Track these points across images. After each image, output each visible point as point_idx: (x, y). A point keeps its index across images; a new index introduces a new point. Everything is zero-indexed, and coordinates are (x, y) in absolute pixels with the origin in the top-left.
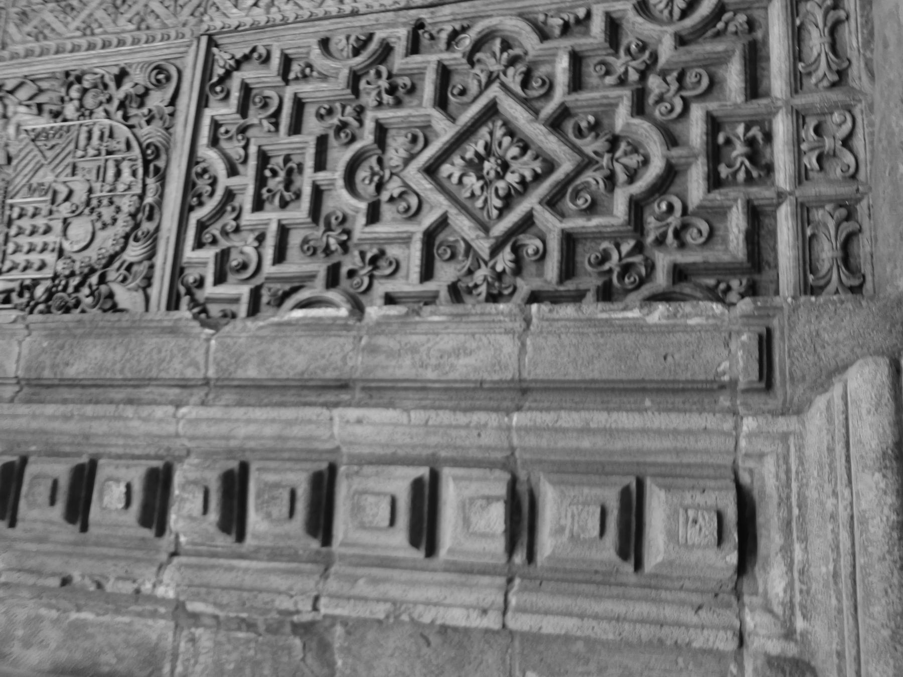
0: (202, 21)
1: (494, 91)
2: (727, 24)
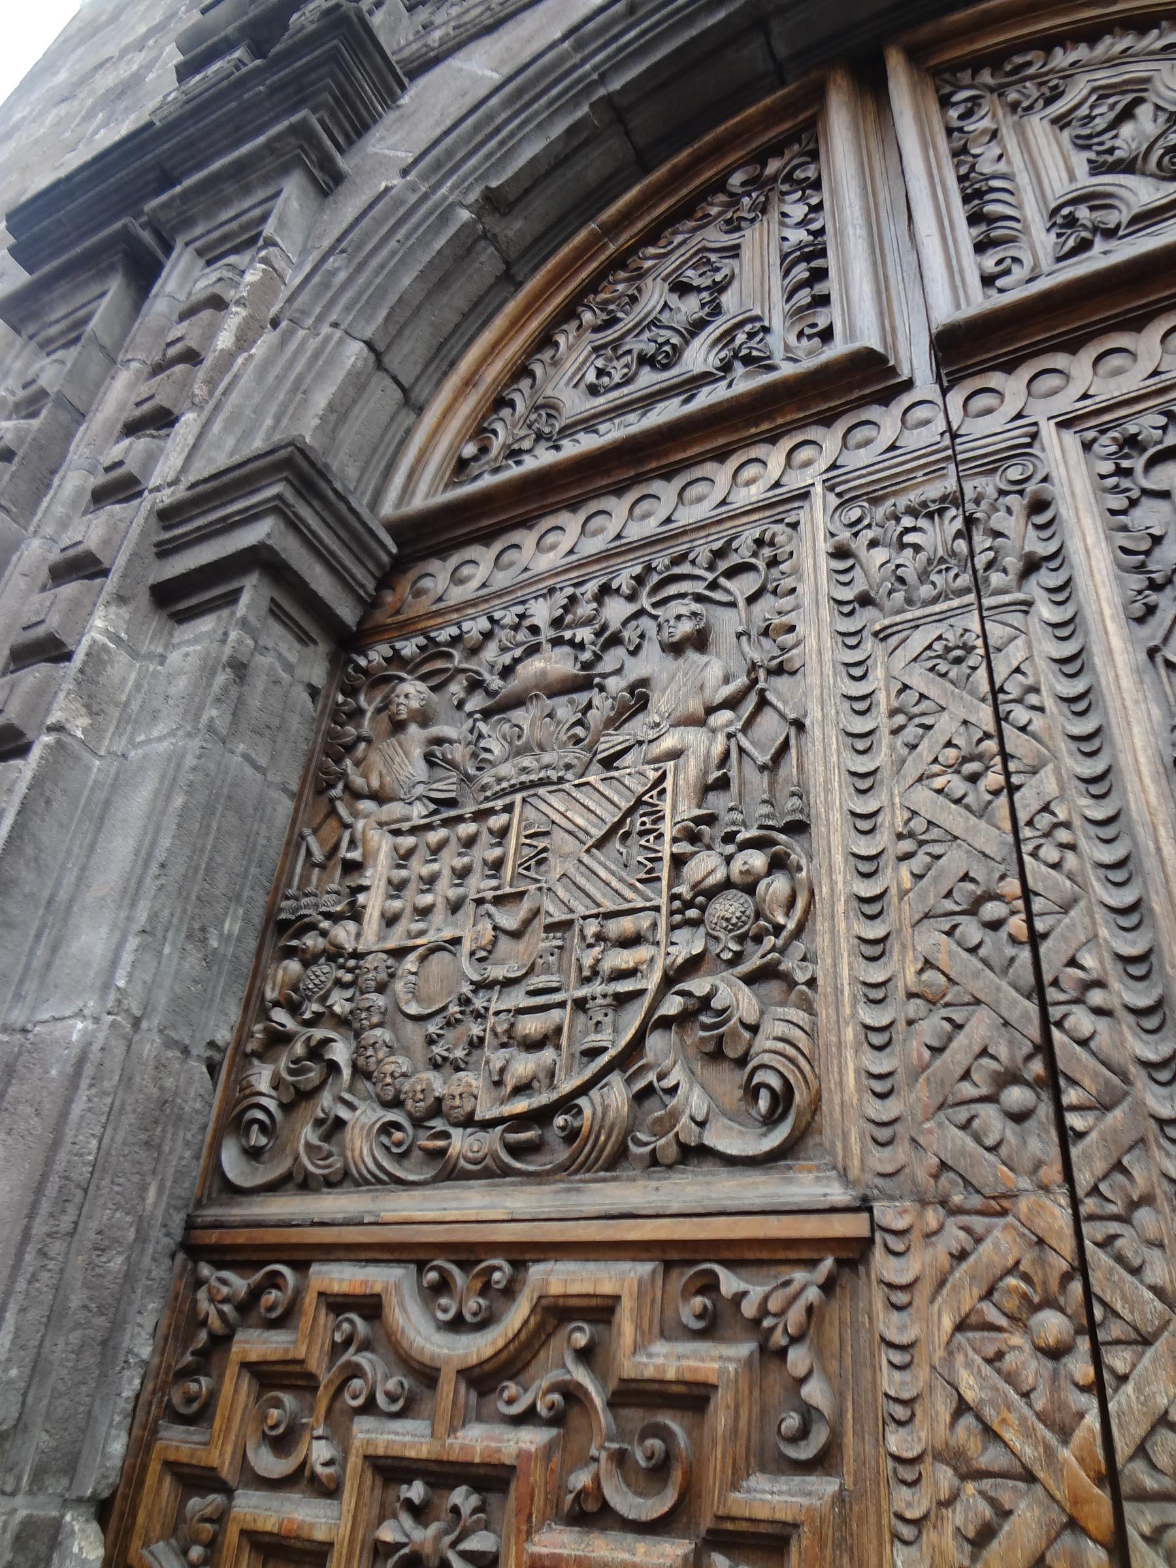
0: (924, 1203)
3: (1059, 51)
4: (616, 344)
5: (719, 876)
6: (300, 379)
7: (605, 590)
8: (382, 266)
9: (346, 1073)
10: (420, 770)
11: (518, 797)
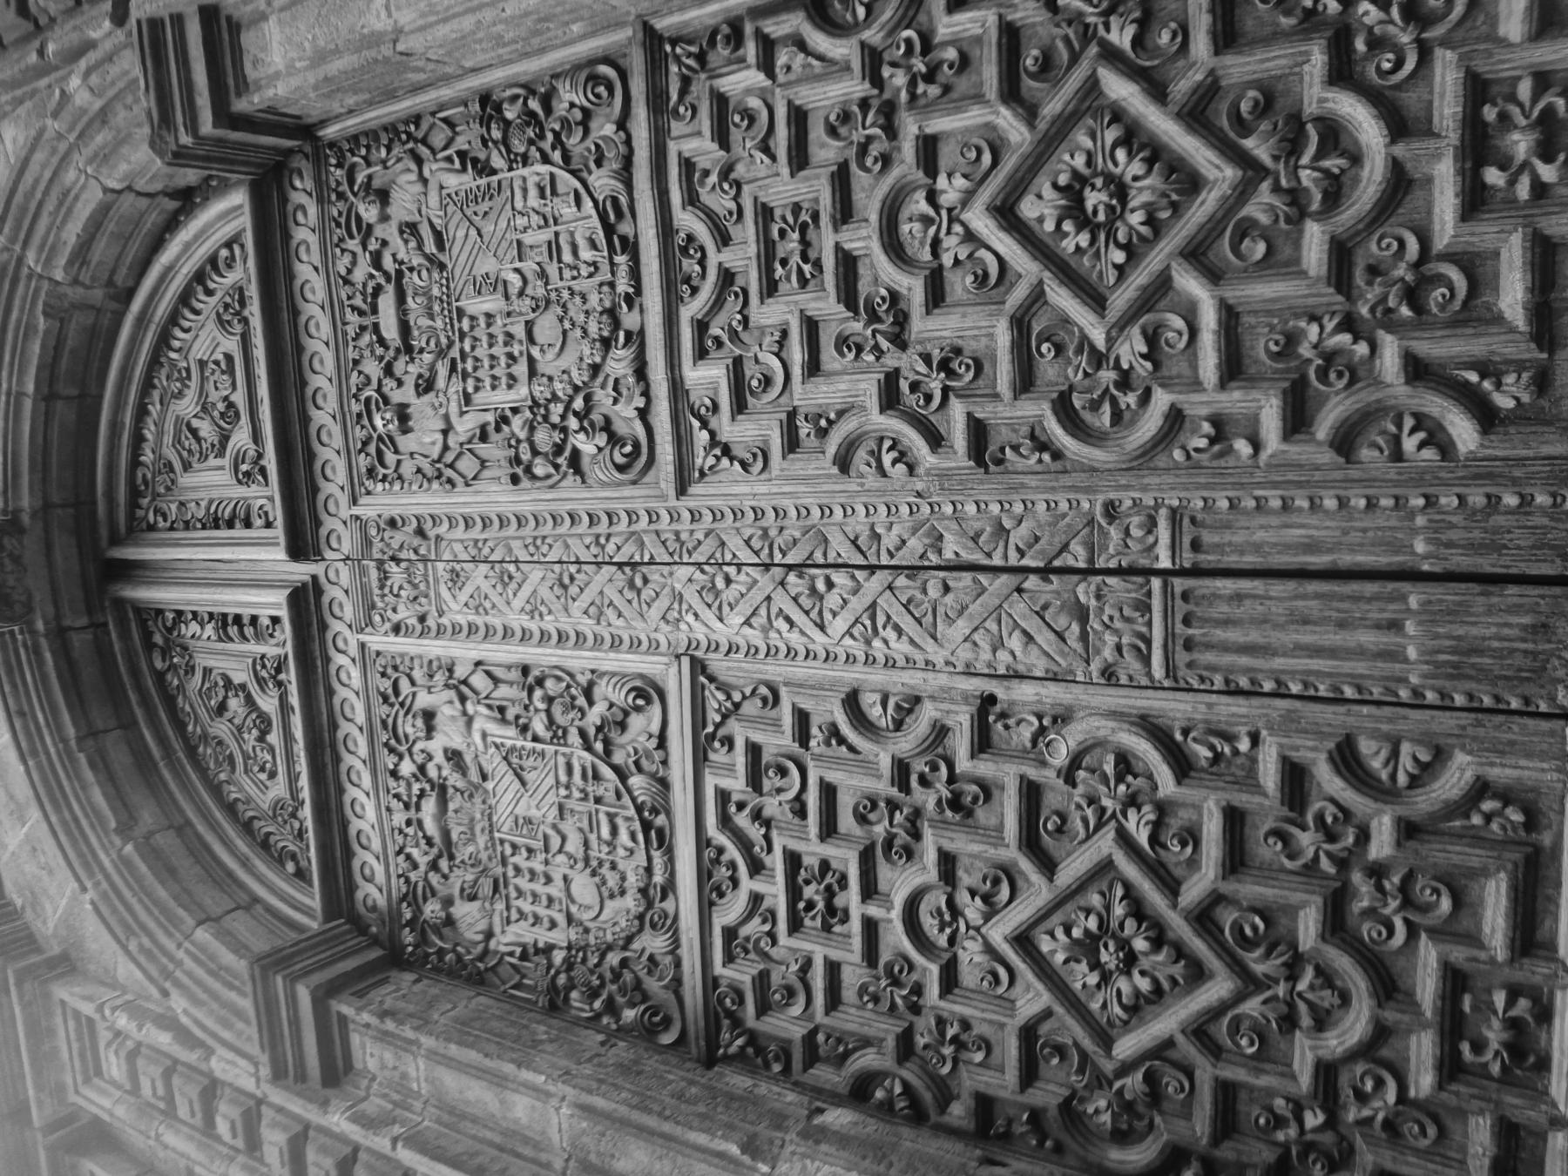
1: (1105, 843)
2: (1488, 818)
3: (142, 458)
4: (246, 757)
5: (543, 715)
6: (211, 972)
7: (394, 774)
8: (147, 909)
9: (628, 954)
10: (477, 904)
11: (497, 835)
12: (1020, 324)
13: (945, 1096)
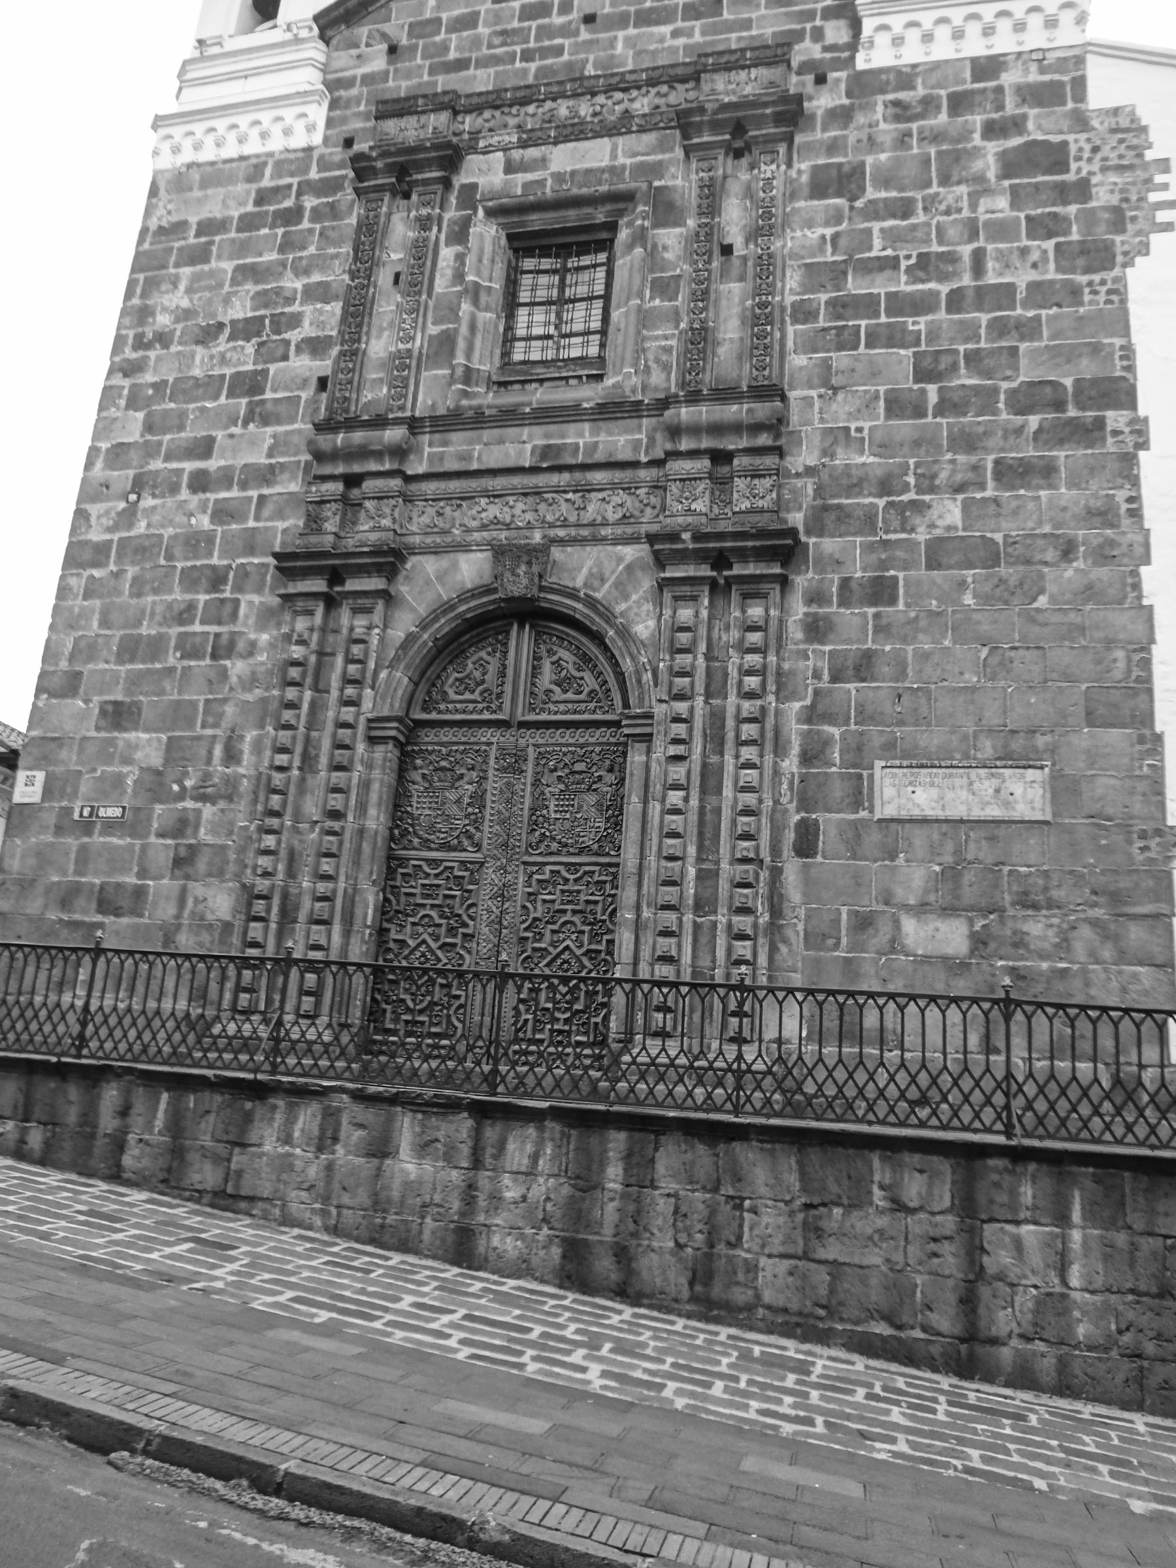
12: (545, 949)
13: (388, 921)
